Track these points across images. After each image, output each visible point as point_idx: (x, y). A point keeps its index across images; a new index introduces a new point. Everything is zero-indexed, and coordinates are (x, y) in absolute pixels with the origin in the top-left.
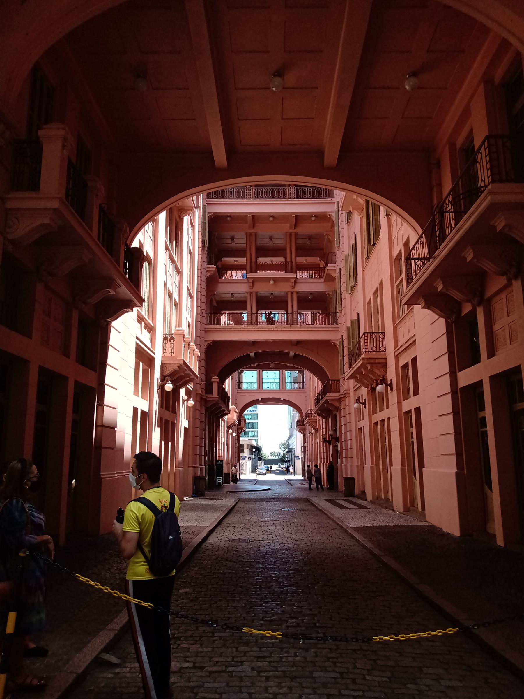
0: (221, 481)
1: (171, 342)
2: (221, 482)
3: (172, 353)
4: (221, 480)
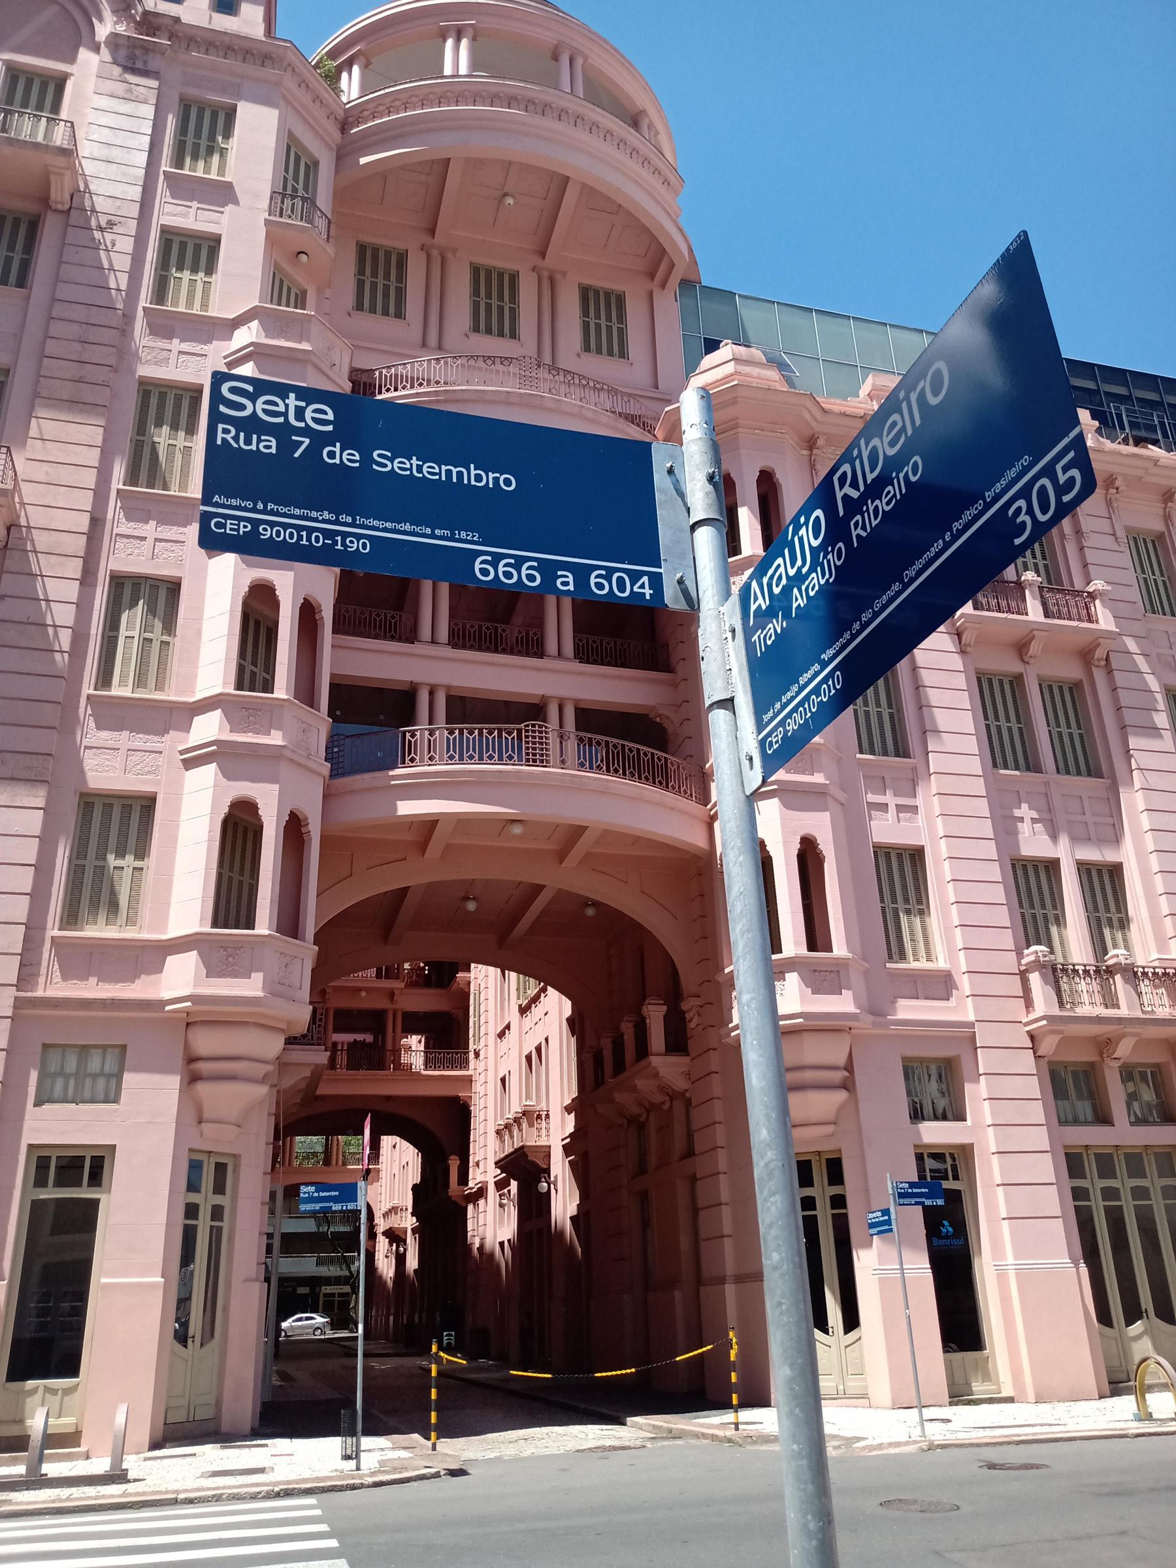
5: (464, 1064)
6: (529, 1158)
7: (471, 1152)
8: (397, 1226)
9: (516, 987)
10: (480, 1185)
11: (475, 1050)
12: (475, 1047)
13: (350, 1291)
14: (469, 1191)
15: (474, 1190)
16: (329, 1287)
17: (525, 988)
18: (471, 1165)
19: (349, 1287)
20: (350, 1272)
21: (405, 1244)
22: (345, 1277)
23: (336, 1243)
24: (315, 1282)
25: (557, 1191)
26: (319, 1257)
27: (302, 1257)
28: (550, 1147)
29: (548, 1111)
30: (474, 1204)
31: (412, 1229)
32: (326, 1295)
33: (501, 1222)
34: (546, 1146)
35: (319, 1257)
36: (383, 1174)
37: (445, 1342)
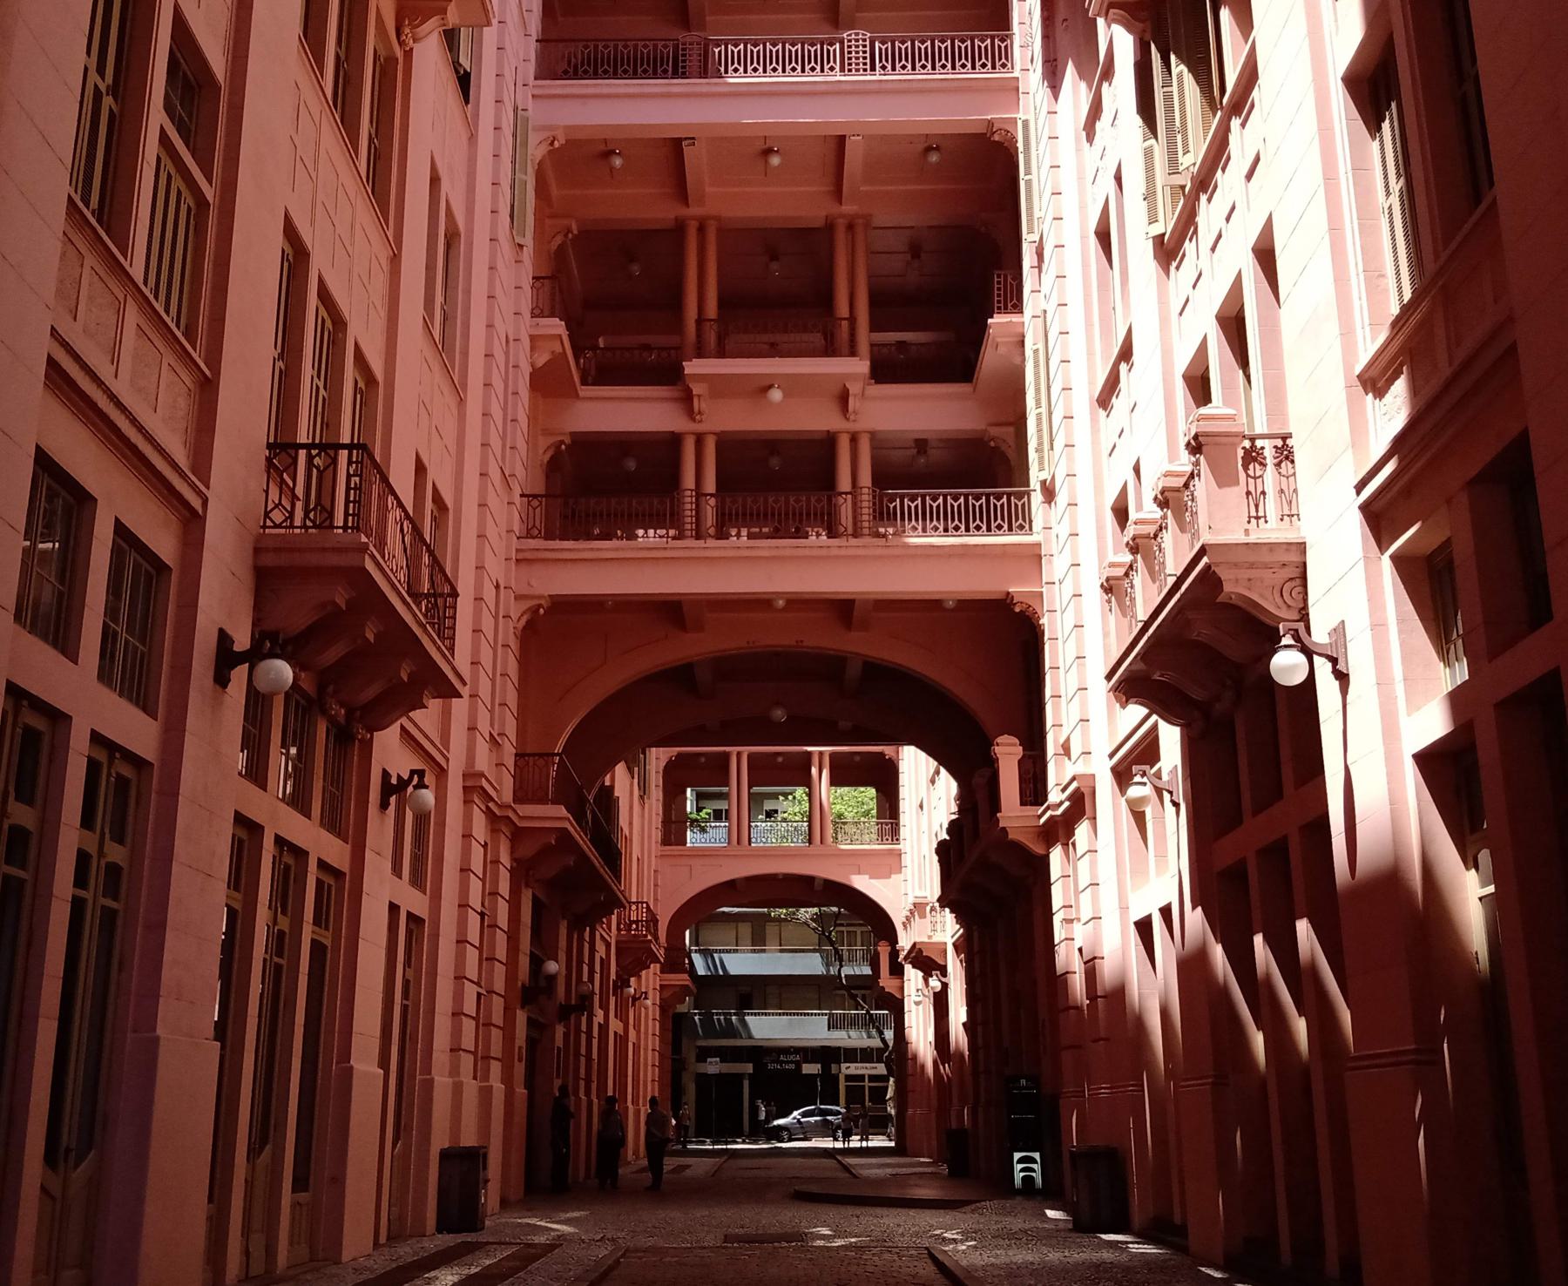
0: (1033, 1171)
1: (1251, 472)
2: (1038, 1176)
3: (1257, 518)
4: (1035, 1166)
5: (1018, 518)
6: (1227, 588)
7: (1049, 722)
8: (926, 940)
9: (1142, 189)
10: (1075, 785)
11: (1043, 483)
12: (1045, 475)
13: (885, 1072)
15: (1059, 812)
17: (1173, 162)
18: (1051, 749)
19: (883, 1065)
20: (883, 1040)
21: (944, 974)
22: (878, 1049)
23: (859, 993)
24: (828, 1055)
25: (1342, 677)
26: (831, 1015)
28: (1301, 547)
29: (1285, 438)
31: (954, 944)
32: (849, 1078)
33: (1139, 871)
34: (1289, 545)
35: (831, 1015)
36: (907, 860)
37: (1018, 1176)
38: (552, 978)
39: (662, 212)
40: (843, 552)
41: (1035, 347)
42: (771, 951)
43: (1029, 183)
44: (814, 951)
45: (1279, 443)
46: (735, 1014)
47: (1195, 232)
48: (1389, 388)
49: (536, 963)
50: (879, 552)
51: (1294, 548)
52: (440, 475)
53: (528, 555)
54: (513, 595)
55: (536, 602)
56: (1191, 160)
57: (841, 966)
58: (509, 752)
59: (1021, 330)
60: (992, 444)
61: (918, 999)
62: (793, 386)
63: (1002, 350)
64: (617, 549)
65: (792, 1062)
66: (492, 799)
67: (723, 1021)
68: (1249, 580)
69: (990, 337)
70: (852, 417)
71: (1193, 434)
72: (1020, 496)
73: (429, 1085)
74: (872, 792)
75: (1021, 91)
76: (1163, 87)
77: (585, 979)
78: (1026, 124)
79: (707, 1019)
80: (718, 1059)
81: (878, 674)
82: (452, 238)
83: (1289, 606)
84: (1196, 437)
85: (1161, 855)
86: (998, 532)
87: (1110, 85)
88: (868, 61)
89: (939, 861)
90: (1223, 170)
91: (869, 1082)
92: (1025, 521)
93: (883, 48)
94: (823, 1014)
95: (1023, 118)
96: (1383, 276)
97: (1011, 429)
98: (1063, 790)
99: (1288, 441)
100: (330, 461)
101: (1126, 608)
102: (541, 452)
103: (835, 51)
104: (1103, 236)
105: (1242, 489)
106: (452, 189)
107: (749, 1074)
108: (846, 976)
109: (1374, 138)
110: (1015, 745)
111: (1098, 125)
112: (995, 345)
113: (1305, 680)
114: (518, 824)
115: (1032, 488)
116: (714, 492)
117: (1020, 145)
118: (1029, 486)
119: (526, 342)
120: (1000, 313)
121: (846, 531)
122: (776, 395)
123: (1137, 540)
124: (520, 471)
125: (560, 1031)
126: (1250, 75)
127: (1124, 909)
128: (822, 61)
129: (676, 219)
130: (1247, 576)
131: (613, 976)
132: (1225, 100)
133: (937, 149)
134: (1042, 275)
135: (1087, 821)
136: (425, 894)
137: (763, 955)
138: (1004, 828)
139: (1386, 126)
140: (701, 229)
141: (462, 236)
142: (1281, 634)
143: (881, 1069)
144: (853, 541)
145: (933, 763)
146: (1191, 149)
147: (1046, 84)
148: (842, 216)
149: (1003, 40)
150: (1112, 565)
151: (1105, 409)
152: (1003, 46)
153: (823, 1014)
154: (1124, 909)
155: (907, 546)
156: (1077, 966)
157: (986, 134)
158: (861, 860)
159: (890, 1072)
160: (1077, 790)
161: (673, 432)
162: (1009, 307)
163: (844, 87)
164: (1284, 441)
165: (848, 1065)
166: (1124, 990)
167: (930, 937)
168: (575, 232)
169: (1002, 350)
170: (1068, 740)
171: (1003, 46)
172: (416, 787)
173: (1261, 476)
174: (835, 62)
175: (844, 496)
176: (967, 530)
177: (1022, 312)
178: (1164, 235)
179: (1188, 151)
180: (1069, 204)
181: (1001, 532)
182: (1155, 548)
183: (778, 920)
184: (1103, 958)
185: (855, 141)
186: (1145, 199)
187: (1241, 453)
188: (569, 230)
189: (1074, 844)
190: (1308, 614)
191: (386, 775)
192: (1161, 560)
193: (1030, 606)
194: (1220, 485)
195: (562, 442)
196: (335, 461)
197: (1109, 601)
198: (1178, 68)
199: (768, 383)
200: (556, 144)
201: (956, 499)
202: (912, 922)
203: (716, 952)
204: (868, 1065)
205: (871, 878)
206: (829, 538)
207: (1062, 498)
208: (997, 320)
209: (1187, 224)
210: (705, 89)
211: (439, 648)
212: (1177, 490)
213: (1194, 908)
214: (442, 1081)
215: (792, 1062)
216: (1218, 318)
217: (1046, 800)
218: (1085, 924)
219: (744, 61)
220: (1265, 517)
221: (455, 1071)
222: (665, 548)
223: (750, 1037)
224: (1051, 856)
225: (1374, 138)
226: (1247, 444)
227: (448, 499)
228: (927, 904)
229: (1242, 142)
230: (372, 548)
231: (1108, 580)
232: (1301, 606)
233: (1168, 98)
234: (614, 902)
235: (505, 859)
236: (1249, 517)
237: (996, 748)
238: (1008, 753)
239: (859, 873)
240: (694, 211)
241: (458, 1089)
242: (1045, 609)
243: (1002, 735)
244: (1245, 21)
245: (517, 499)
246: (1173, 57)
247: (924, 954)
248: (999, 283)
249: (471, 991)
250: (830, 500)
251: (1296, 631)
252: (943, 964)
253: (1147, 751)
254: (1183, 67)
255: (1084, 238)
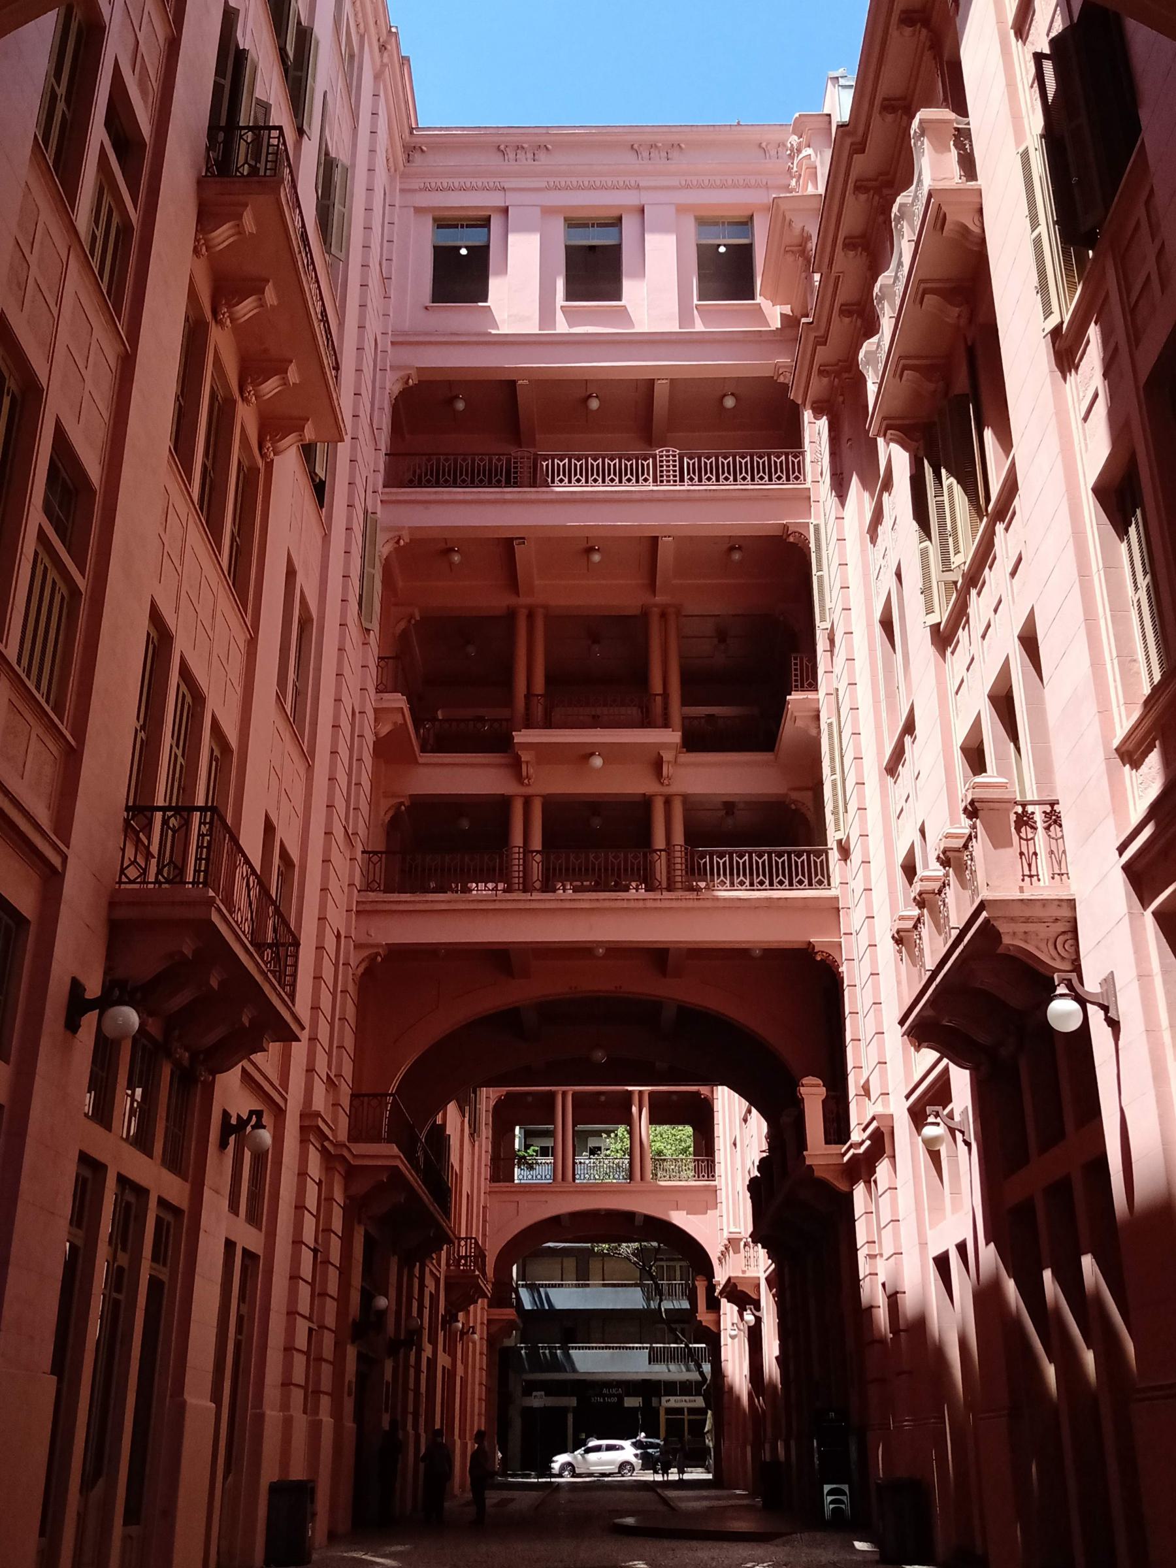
1: (1023, 835)
3: (1031, 876)
5: (818, 874)
6: (1006, 940)
8: (741, 1275)
10: (874, 1124)
11: (840, 842)
12: (840, 835)
14: (852, 1152)
16: (672, 1399)
18: (852, 1091)
19: (701, 1398)
20: (702, 1374)
21: (758, 1308)
22: (697, 1382)
23: (678, 1326)
24: (649, 1389)
25: (1114, 1025)
26: (651, 1348)
27: (627, 1348)
28: (1072, 903)
29: (1053, 804)
30: (868, 1182)
31: (767, 1279)
32: (669, 1411)
33: (937, 1208)
34: (1060, 902)
35: (651, 1348)
36: (722, 1196)
38: (382, 1314)
39: (495, 601)
40: (658, 904)
41: (829, 721)
42: (595, 1285)
43: (820, 578)
44: (636, 1285)
45: (1048, 809)
46: (559, 1348)
47: (967, 621)
48: (1144, 760)
49: (367, 1298)
50: (690, 904)
51: (1064, 904)
52: (287, 834)
53: (368, 907)
54: (352, 943)
55: (375, 951)
56: (962, 559)
57: (661, 1300)
58: (345, 1090)
59: (816, 706)
60: (793, 807)
61: (734, 1333)
62: (613, 754)
63: (799, 723)
64: (449, 902)
65: (614, 1395)
66: (327, 1138)
67: (548, 1355)
68: (1025, 933)
69: (790, 711)
70: (666, 782)
71: (969, 800)
72: (818, 854)
73: (260, 1418)
74: (689, 1130)
75: (812, 500)
76: (935, 497)
77: (415, 1314)
78: (817, 528)
79: (533, 1352)
80: (543, 1393)
81: (689, 1016)
82: (305, 622)
83: (1063, 958)
84: (972, 803)
85: (956, 1192)
86: (799, 887)
87: (890, 495)
88: (677, 473)
89: (751, 1198)
90: (991, 568)
91: (688, 1414)
92: (823, 877)
93: (691, 462)
94: (643, 1348)
95: (815, 522)
96: (1135, 661)
97: (810, 793)
98: (864, 1130)
99: (1056, 807)
100: (183, 822)
101: (916, 959)
102: (382, 813)
103: (648, 464)
104: (887, 624)
105: (1014, 851)
106: (307, 582)
107: (574, 1408)
108: (665, 1310)
109: (1122, 540)
110: (818, 1086)
111: (880, 529)
112: (793, 719)
113: (1078, 1029)
114: (352, 1162)
115: (829, 846)
116: (540, 849)
117: (812, 546)
118: (827, 845)
119: (371, 714)
120: (797, 691)
121: (660, 884)
122: (597, 762)
123: (924, 895)
124: (362, 830)
125: (389, 1365)
126: (1011, 487)
127: (923, 1245)
128: (637, 475)
129: (508, 607)
130: (1022, 930)
131: (442, 1311)
132: (990, 509)
133: (740, 548)
134: (834, 658)
135: (887, 1159)
136: (260, 1230)
137: (588, 1289)
138: (810, 1166)
139: (1132, 530)
140: (531, 616)
141: (315, 623)
142: (1056, 983)
143: (699, 1402)
144: (666, 895)
145: (745, 1104)
146: (962, 549)
147: (834, 494)
148: (656, 605)
149: (796, 457)
150: (902, 918)
151: (892, 776)
152: (796, 461)
153: (643, 1348)
154: (923, 1245)
155: (717, 899)
156: (881, 1300)
157: (782, 536)
158: (680, 1197)
159: (708, 1406)
160: (877, 1129)
161: (503, 795)
162: (806, 686)
163: (656, 496)
164: (1052, 807)
165: (668, 1398)
166: (925, 1323)
167: (744, 1272)
168: (418, 618)
169: (799, 723)
170: (868, 1081)
171: (796, 461)
172: (254, 1127)
173: (1032, 839)
174: (648, 474)
175: (658, 853)
176: (771, 884)
177: (817, 690)
178: (939, 624)
179: (959, 552)
180: (856, 597)
181: (802, 887)
182: (940, 903)
183: (602, 1255)
184: (904, 1293)
185: (668, 541)
186: (922, 593)
187: (1013, 817)
188: (412, 617)
189: (875, 1182)
190: (1080, 965)
191: (226, 1115)
192: (946, 914)
193: (830, 955)
194: (995, 847)
195: (402, 803)
196: (187, 824)
197: (900, 952)
198: (948, 480)
199: (589, 751)
200: (402, 542)
201: (760, 856)
202: (727, 1257)
203: (542, 1287)
204: (687, 1398)
205: (687, 1214)
206: (646, 891)
207: (856, 856)
208: (794, 697)
209: (960, 614)
210: (533, 497)
211: (279, 995)
212: (958, 850)
213: (987, 1244)
214: (272, 1414)
215: (614, 1395)
216: (990, 697)
217: (849, 1138)
218: (887, 1260)
219: (569, 473)
220: (1038, 875)
221: (285, 1406)
222: (495, 900)
223: (574, 1370)
224: (855, 1192)
225: (1122, 540)
226: (1019, 809)
227: (295, 855)
228: (741, 1239)
229: (1006, 544)
230: (218, 902)
231: (898, 932)
232: (1074, 957)
233: (940, 506)
234: (442, 1237)
235: (338, 1196)
236: (1023, 875)
237: (801, 1088)
238: (813, 1094)
239: (677, 1210)
240: (524, 600)
241: (288, 1422)
242: (844, 958)
243: (807, 1076)
244: (1005, 440)
245: (359, 856)
246: (943, 471)
247: (739, 1288)
248: (796, 664)
249: (302, 1326)
250: (645, 856)
251: (1070, 980)
252: (755, 1297)
253: (940, 1093)
254: (952, 480)
255: (869, 625)
